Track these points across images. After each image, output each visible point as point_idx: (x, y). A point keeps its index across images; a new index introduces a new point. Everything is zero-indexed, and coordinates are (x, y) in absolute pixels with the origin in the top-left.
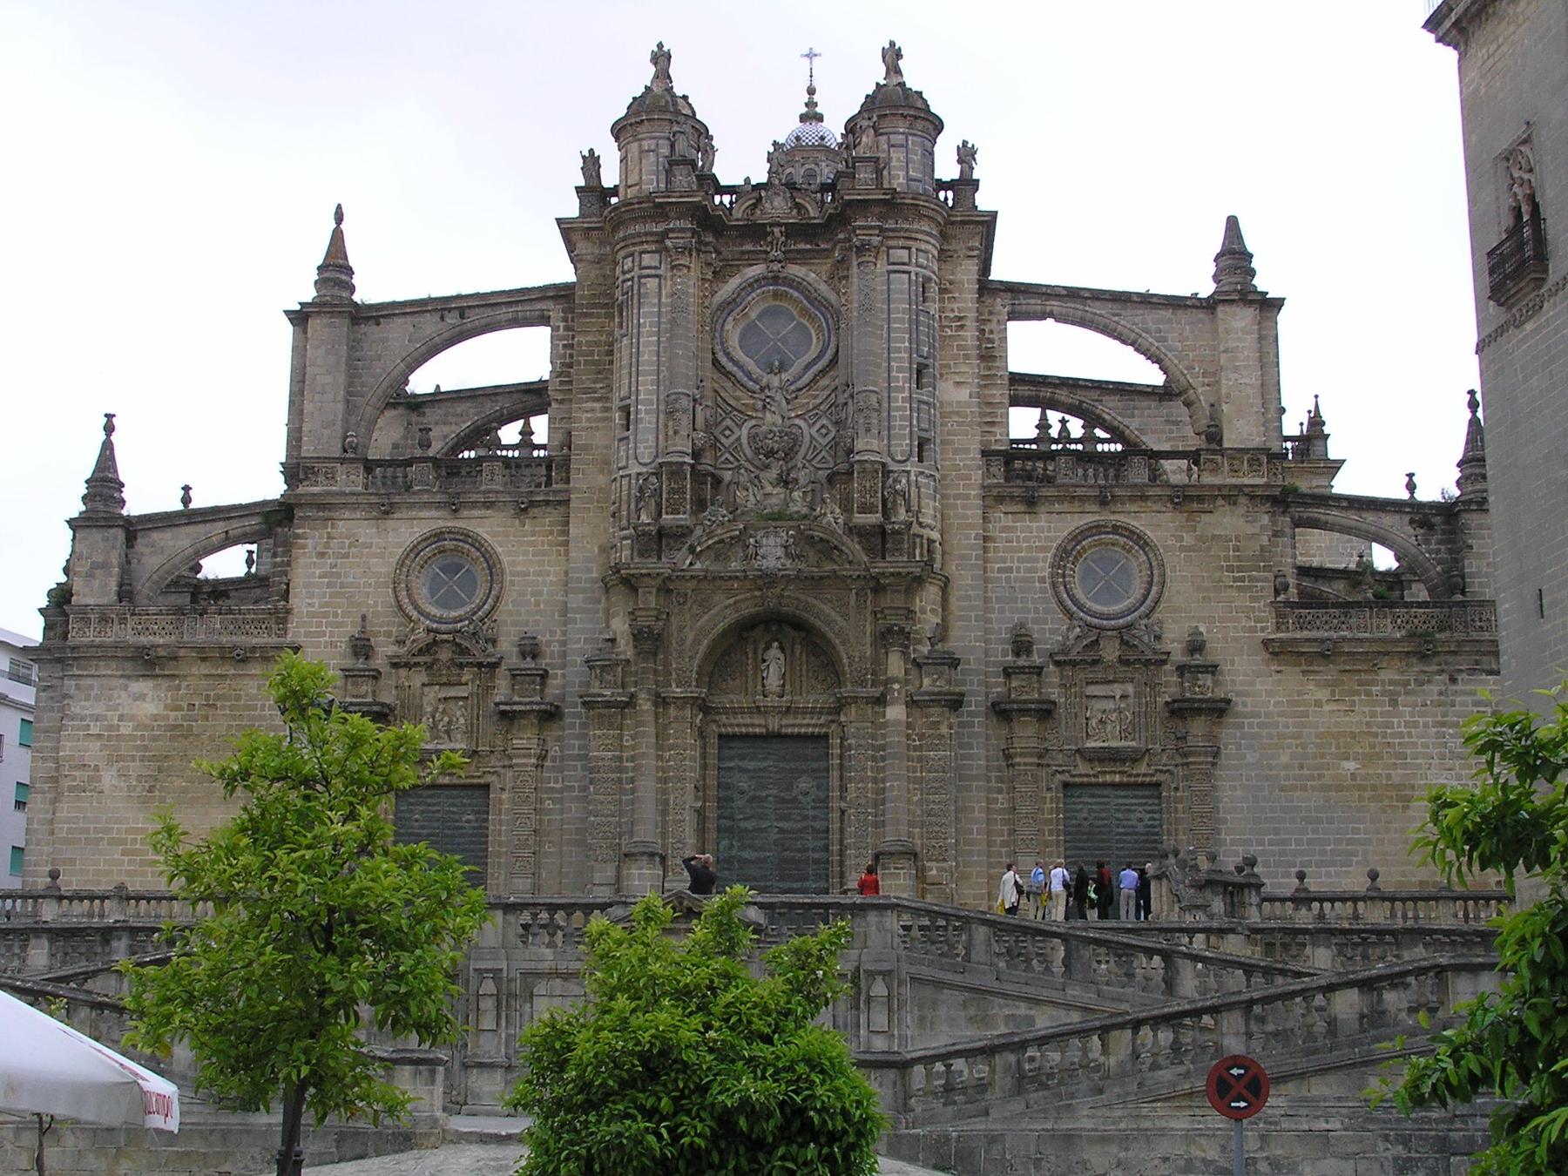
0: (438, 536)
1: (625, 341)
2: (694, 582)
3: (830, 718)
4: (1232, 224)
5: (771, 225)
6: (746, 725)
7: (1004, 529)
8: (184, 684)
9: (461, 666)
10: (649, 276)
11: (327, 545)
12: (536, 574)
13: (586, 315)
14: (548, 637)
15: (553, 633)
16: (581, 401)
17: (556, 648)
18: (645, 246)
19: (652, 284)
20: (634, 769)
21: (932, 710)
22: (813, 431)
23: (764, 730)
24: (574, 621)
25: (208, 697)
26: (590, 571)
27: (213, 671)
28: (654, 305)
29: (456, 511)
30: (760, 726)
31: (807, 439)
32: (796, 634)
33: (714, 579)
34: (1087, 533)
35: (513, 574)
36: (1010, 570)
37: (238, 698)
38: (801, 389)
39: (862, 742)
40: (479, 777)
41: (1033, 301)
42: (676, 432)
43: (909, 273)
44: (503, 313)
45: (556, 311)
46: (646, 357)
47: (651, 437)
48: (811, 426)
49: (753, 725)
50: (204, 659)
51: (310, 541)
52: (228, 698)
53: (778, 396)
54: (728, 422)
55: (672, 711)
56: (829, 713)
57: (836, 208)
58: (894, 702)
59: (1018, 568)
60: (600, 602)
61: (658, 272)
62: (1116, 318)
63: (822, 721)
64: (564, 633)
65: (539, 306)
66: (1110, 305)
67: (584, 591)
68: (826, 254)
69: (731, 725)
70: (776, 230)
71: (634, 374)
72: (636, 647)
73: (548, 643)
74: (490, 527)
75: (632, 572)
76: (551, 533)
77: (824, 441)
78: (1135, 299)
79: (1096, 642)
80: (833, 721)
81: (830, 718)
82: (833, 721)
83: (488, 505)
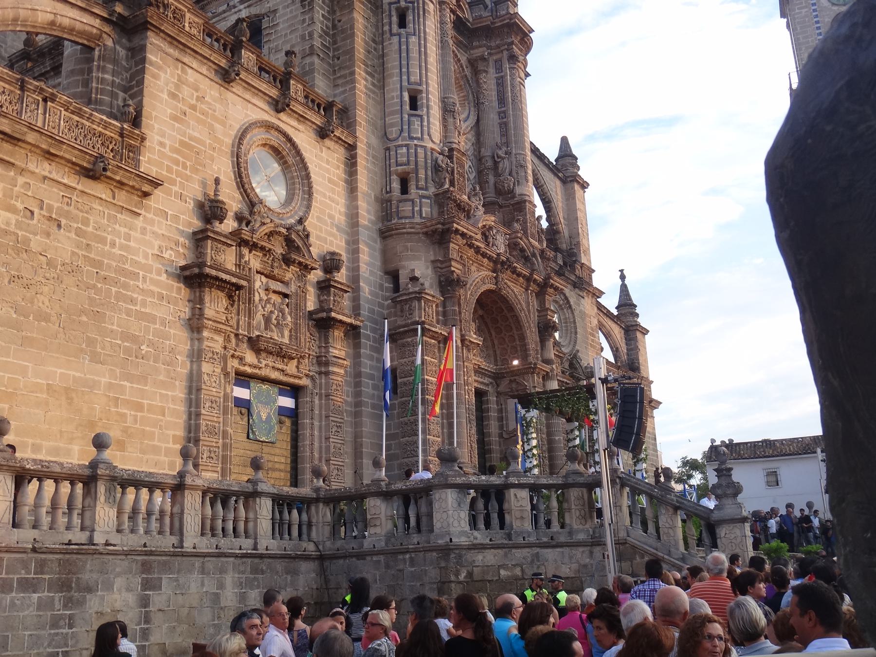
0: (269, 126)
1: (413, 39)
4: (564, 141)
8: (21, 180)
9: (287, 261)
11: (177, 87)
19: (431, 6)
25: (50, 208)
27: (54, 176)
29: (278, 111)
35: (317, 190)
37: (86, 222)
40: (300, 378)
50: (49, 156)
51: (162, 75)
52: (74, 219)
56: (489, 377)
63: (485, 381)
71: (424, 68)
74: (304, 138)
75: (459, 227)
81: (491, 380)
82: (491, 383)
83: (302, 118)
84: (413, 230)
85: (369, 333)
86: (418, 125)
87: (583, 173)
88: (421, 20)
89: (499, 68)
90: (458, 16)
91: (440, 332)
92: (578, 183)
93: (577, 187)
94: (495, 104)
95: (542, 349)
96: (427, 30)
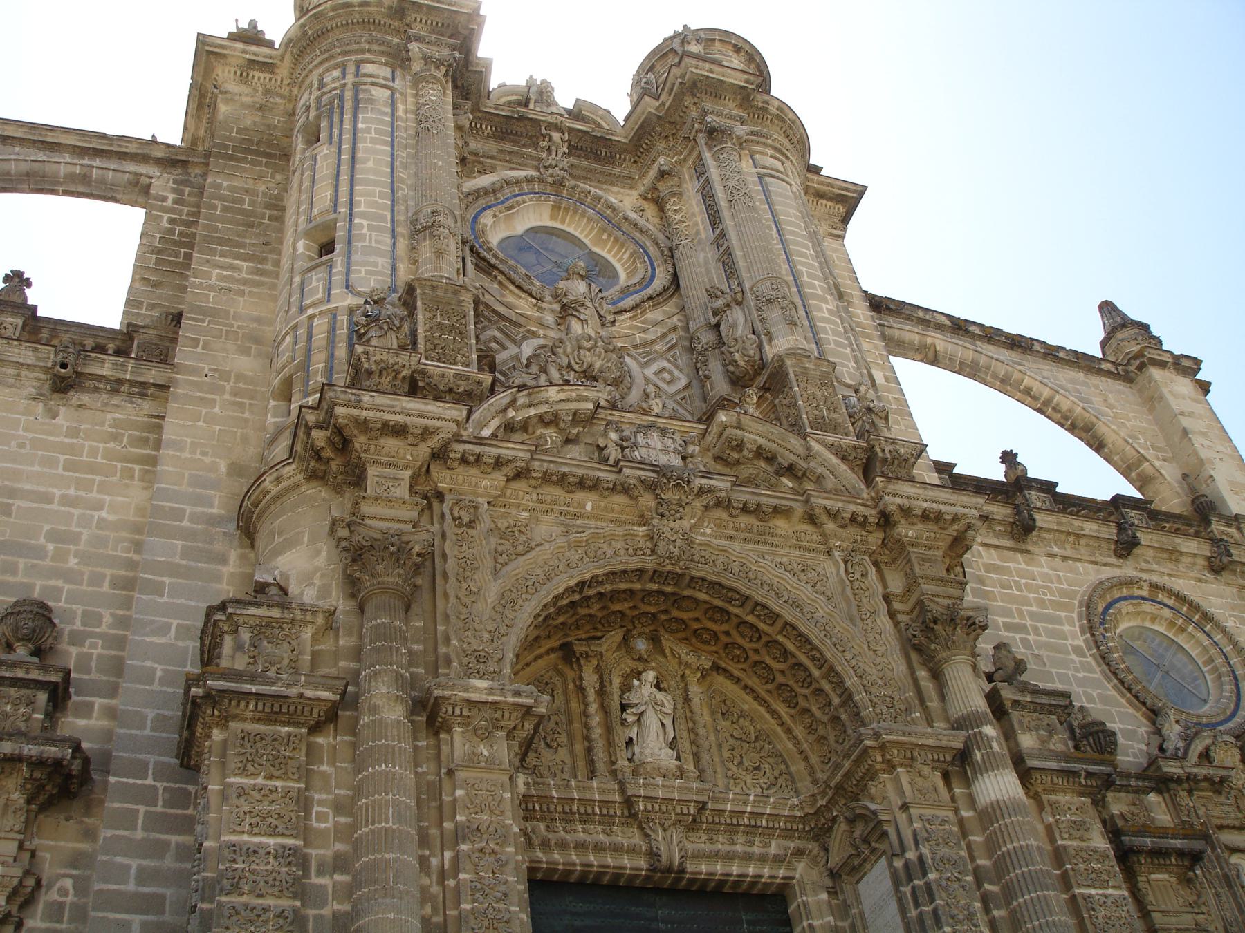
2: (499, 477)
3: (792, 845)
4: (1107, 308)
5: (550, 126)
6: (599, 848)
7: (990, 568)
10: (373, 84)
12: (66, 501)
13: (231, 158)
14: (78, 625)
15: (91, 618)
16: (212, 252)
17: (97, 650)
18: (368, 56)
19: (382, 94)
20: (348, 892)
21: (1063, 798)
22: (649, 372)
23: (643, 863)
24: (158, 589)
26: (205, 501)
28: (386, 114)
30: (632, 851)
31: (639, 380)
32: (692, 659)
33: (546, 478)
34: (1117, 594)
36: (1021, 628)
38: (620, 312)
39: (943, 851)
41: (907, 327)
42: (438, 253)
43: (791, 185)
44: (64, 164)
45: (162, 182)
46: (370, 164)
47: (383, 262)
48: (645, 365)
49: (617, 849)
53: (588, 304)
54: (497, 334)
55: (458, 743)
56: (787, 834)
57: (657, 109)
58: (991, 764)
59: (1036, 630)
60: (223, 560)
61: (391, 84)
62: (1020, 368)
63: (774, 849)
64: (123, 622)
65: (132, 167)
66: (1006, 352)
67: (190, 535)
68: (627, 181)
69: (563, 845)
70: (556, 136)
72: (352, 586)
73: (77, 638)
75: (364, 413)
76: (115, 438)
77: (672, 389)
78: (1037, 347)
79: (1207, 749)
80: (799, 853)
81: (792, 845)
82: (799, 853)
84: (283, 485)
85: (149, 781)
86: (318, 280)
87: (1174, 343)
88: (348, 117)
89: (700, 171)
90: (571, 130)
91: (294, 691)
92: (1162, 365)
93: (1155, 373)
94: (705, 232)
95: (942, 697)
96: (360, 125)
